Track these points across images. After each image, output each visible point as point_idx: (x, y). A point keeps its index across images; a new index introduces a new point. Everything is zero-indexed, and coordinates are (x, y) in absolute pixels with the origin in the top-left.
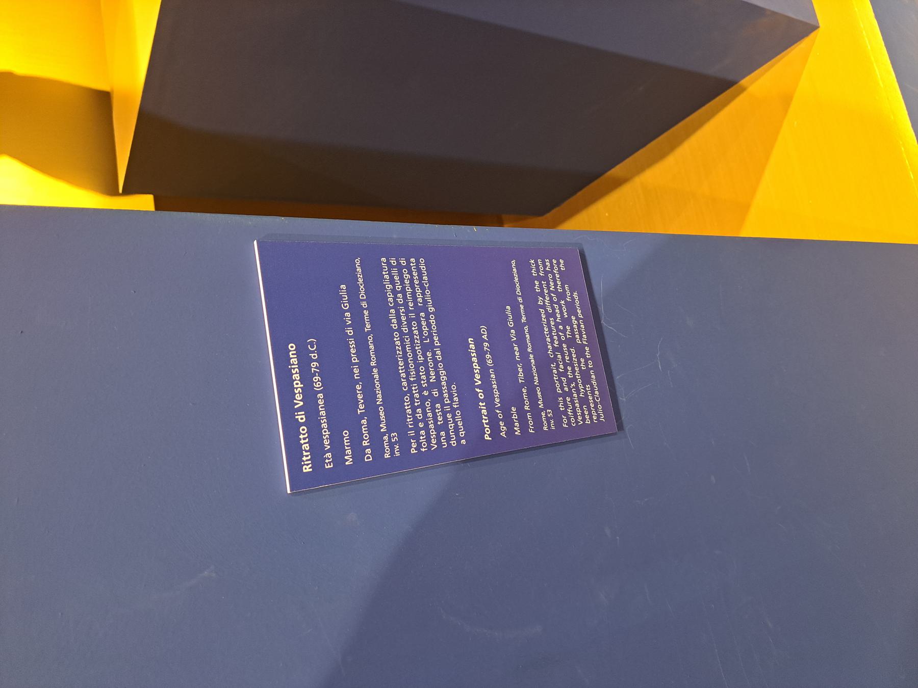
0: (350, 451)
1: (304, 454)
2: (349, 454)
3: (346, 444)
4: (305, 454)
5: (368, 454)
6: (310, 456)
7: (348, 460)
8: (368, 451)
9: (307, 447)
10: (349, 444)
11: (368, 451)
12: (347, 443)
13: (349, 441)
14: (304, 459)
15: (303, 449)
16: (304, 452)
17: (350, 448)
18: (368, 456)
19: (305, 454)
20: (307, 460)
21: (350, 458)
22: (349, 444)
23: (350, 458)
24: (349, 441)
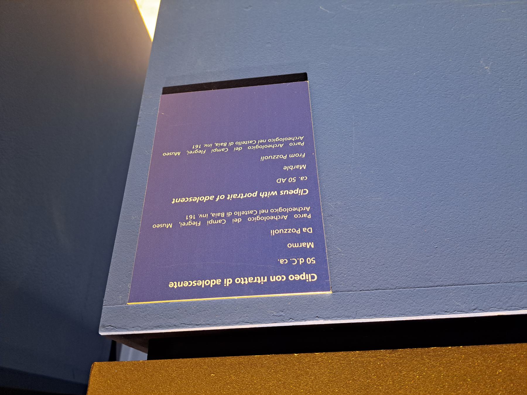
0: (303, 243)
1: (256, 282)
2: (306, 244)
3: (298, 246)
4: (255, 281)
5: (307, 230)
6: (258, 277)
7: (310, 245)
8: (304, 230)
9: (251, 279)
10: (298, 244)
11: (304, 230)
12: (297, 246)
13: (295, 244)
14: (259, 282)
15: (252, 282)
16: (254, 282)
17: (301, 243)
18: (309, 230)
19: (255, 281)
20: (261, 280)
21: (309, 244)
22: (298, 244)
23: (309, 244)
24: (295, 244)
